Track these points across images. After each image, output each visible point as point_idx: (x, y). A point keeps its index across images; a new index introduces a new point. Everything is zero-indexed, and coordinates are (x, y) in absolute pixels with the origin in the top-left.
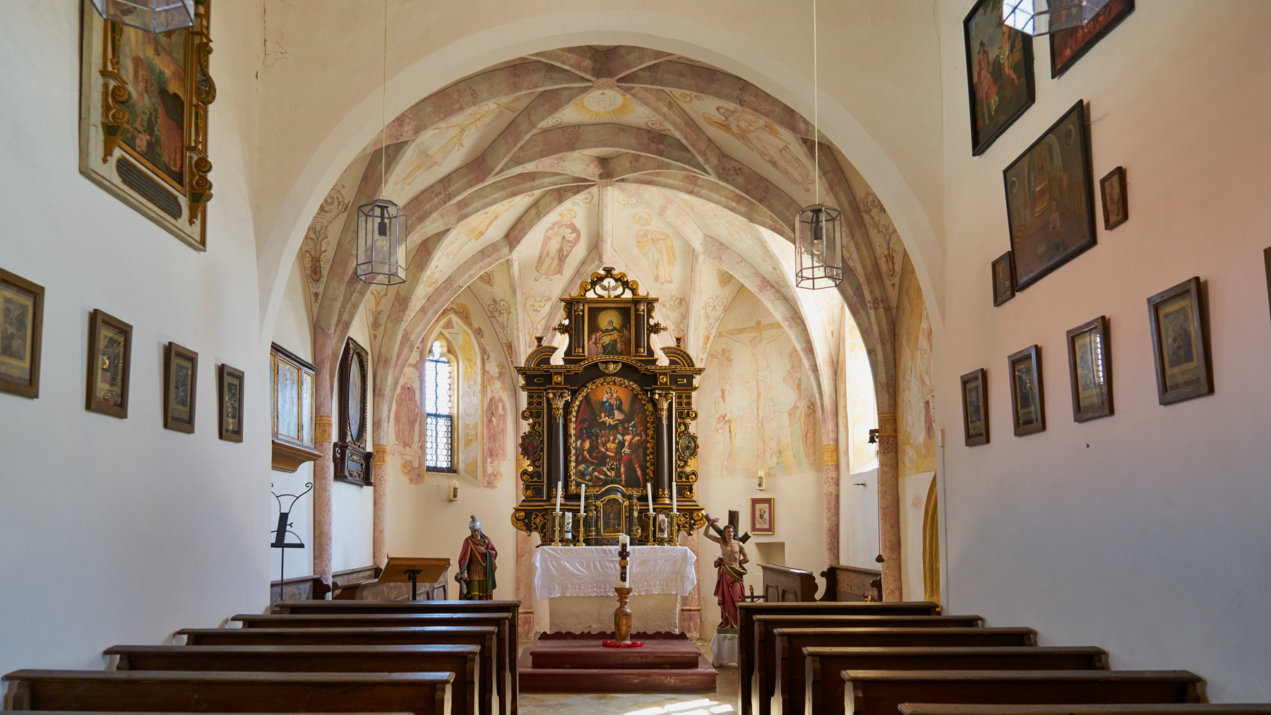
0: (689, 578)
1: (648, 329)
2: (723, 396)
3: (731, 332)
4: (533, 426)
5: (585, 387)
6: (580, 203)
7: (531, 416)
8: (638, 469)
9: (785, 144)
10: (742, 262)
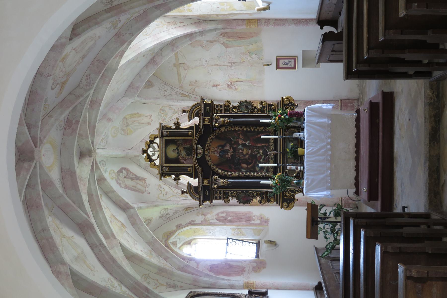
1: (177, 129)
4: (233, 197)
5: (211, 166)
6: (105, 168)
7: (227, 198)
10: (140, 75)
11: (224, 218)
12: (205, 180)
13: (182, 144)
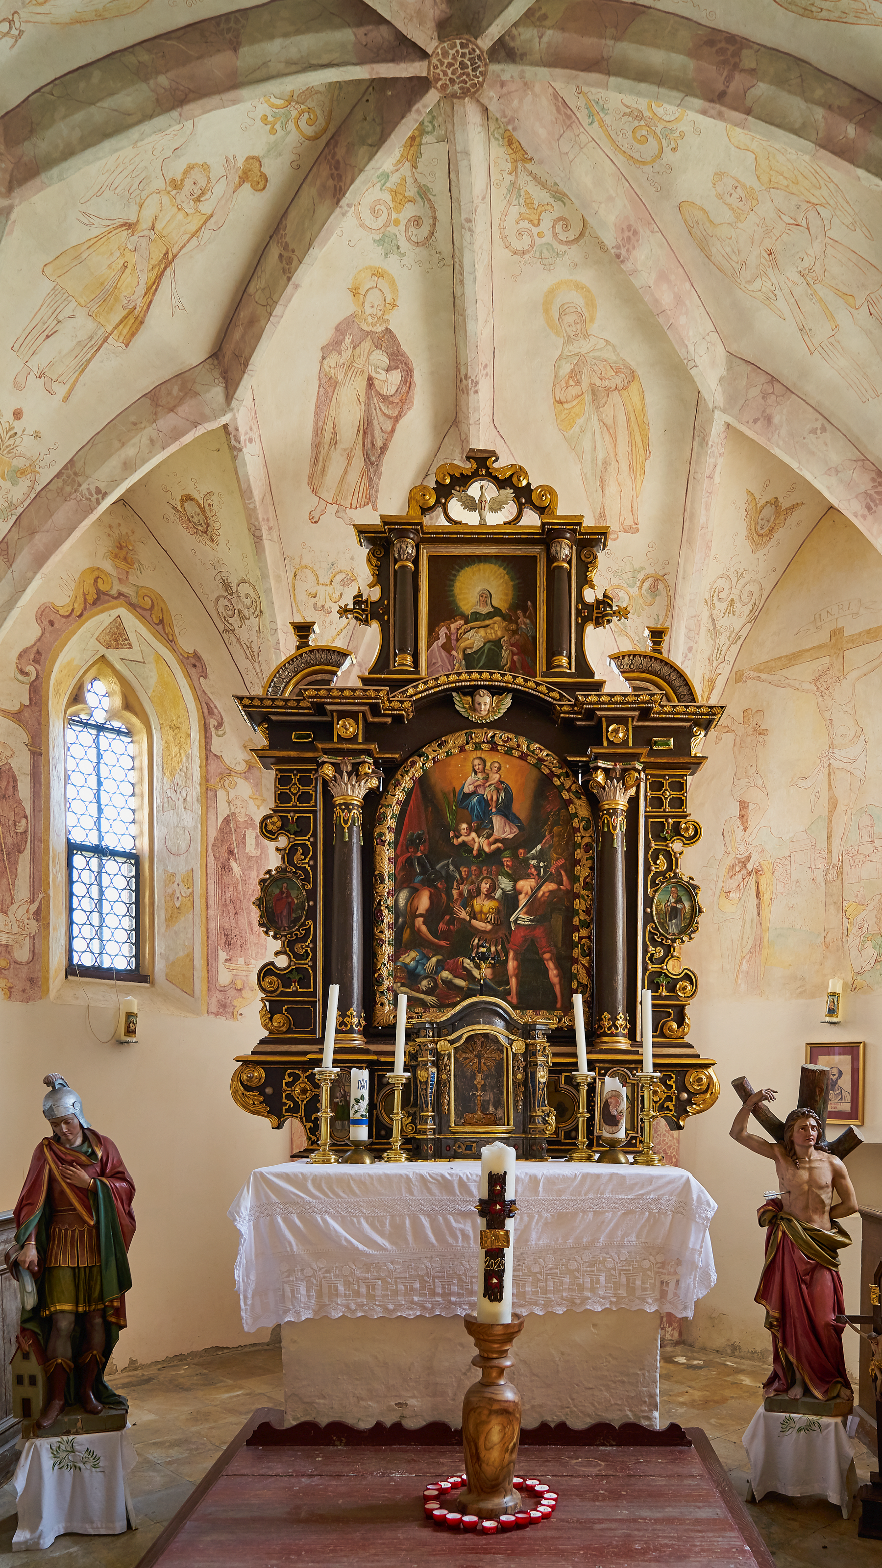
0: (694, 1265)
2: (742, 817)
3: (766, 668)
4: (288, 854)
5: (420, 756)
7: (284, 827)
8: (551, 965)
11: (238, 845)
12: (357, 724)
13: (514, 632)
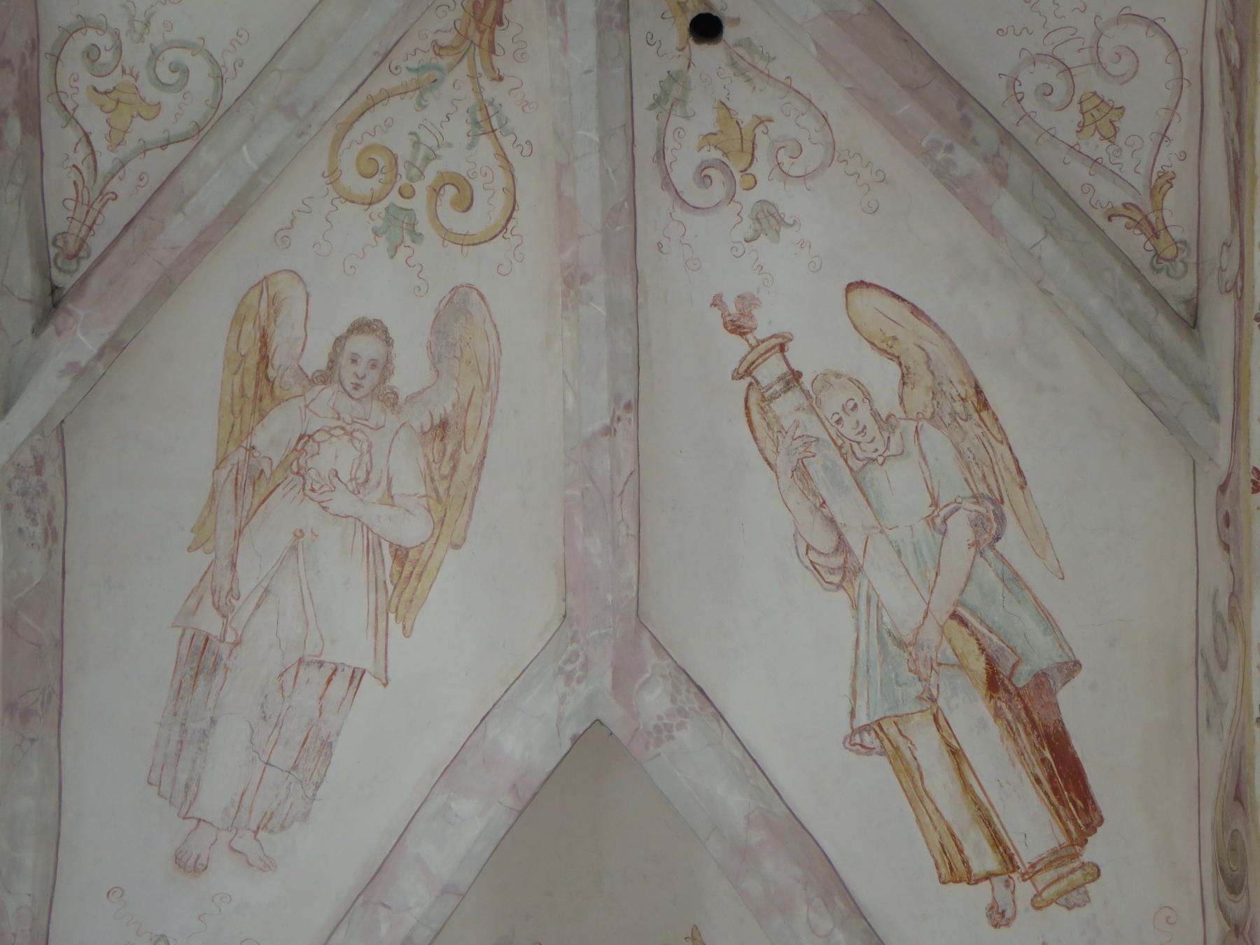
9: (367, 664)
